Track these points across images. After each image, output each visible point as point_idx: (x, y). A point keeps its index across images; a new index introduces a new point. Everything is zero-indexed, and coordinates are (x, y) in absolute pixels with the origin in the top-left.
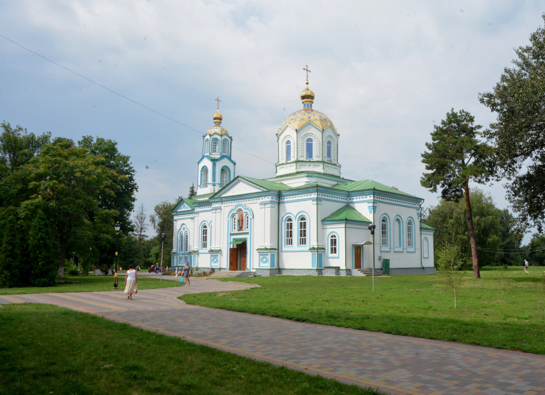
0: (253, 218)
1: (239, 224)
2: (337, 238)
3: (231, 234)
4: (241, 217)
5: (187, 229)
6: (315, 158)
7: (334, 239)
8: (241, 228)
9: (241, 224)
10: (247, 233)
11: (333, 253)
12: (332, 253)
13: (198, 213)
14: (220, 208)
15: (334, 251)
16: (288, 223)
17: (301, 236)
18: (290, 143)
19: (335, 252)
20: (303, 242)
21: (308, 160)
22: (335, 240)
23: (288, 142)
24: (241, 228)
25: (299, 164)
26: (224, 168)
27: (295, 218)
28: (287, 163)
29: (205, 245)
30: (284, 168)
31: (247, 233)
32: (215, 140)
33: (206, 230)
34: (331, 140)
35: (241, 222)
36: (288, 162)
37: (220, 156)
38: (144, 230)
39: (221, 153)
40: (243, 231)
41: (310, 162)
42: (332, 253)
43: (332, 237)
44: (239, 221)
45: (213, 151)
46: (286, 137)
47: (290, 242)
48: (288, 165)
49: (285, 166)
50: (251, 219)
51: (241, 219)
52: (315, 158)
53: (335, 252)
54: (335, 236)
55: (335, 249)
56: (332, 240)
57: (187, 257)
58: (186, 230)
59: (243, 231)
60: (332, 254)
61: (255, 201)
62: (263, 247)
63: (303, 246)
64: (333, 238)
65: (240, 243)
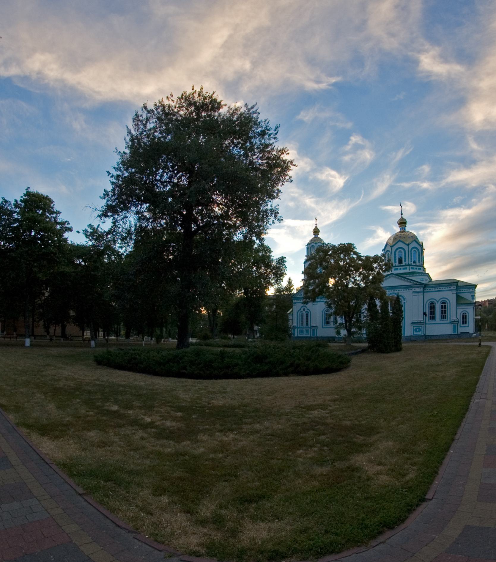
2: (467, 315)
5: (308, 309)
12: (463, 323)
15: (464, 322)
16: (431, 306)
19: (466, 323)
22: (466, 316)
27: (438, 302)
42: (463, 323)
43: (463, 314)
48: (402, 267)
49: (399, 268)
53: (466, 323)
56: (463, 316)
57: (308, 330)
58: (306, 310)
62: (417, 322)
64: (464, 315)
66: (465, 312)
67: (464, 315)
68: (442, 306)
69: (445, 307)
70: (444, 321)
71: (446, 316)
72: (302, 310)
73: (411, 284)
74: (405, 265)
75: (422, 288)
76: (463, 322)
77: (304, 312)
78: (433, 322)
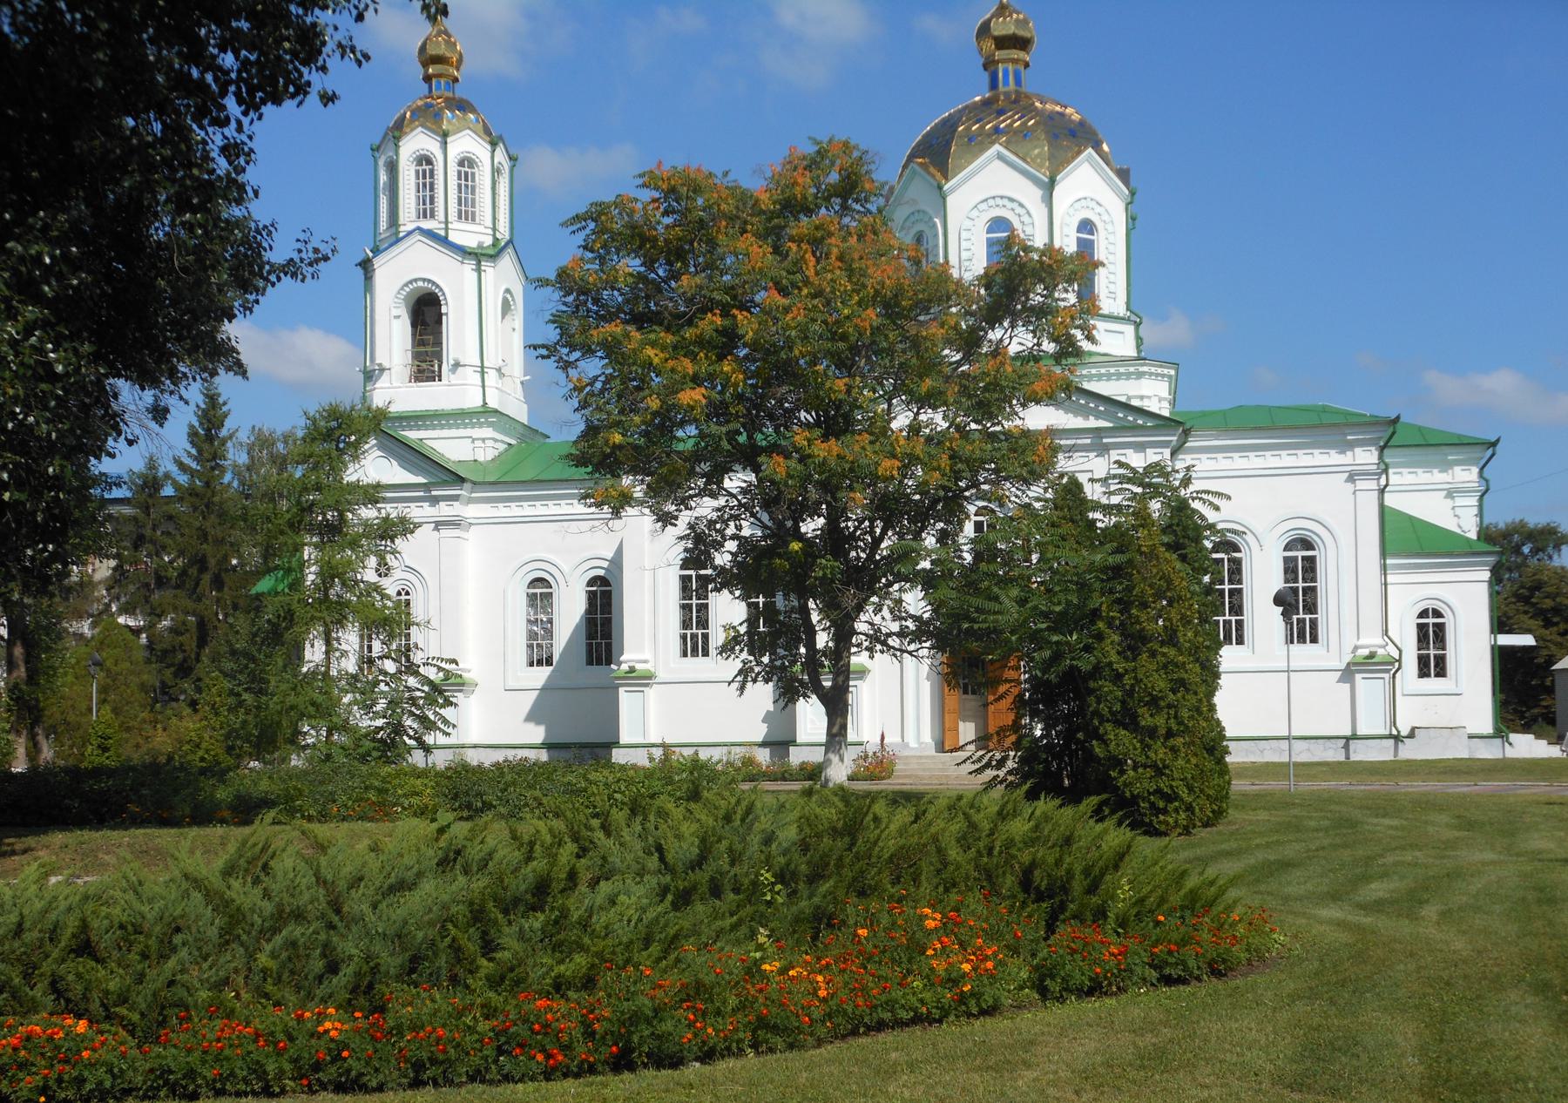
2: (1448, 620)
11: (1428, 675)
12: (1423, 672)
15: (1433, 665)
19: (1441, 672)
20: (1303, 630)
22: (1440, 628)
42: (1423, 672)
43: (1424, 614)
53: (1441, 672)
54: (1437, 614)
56: (1422, 628)
64: (1431, 621)
67: (1431, 621)
70: (1303, 653)
73: (1093, 423)
75: (1167, 452)
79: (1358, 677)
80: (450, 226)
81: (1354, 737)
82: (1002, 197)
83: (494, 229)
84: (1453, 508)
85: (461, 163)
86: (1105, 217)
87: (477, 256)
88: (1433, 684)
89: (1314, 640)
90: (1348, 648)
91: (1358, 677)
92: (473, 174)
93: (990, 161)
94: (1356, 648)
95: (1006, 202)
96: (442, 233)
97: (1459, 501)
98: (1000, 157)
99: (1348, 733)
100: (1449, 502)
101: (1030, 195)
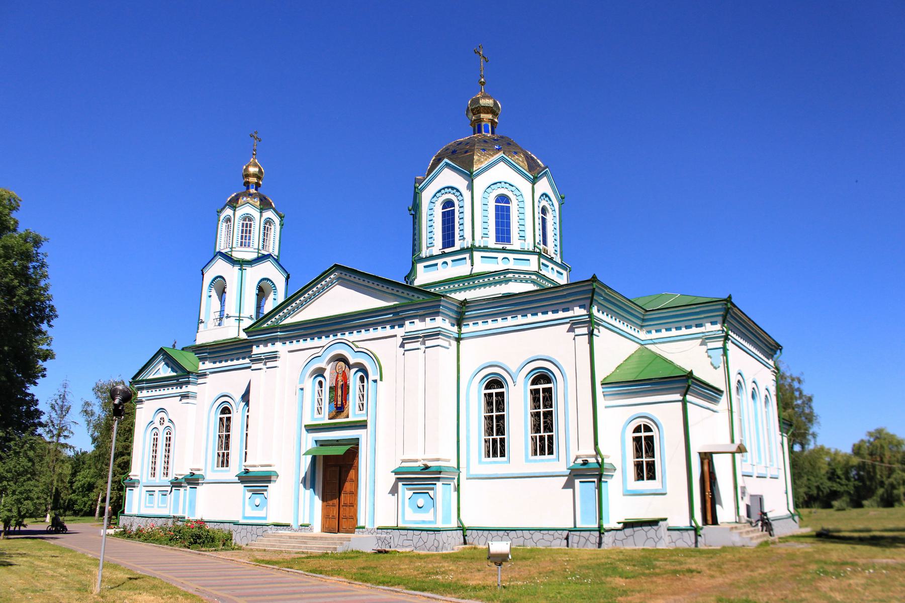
0: (381, 380)
1: (332, 399)
2: (655, 433)
3: (311, 429)
4: (340, 378)
6: (516, 244)
7: (646, 437)
8: (340, 409)
9: (339, 399)
10: (362, 425)
11: (643, 479)
12: (640, 477)
13: (204, 375)
14: (273, 357)
17: (537, 429)
18: (453, 205)
19: (652, 477)
21: (500, 246)
22: (650, 440)
23: (448, 204)
24: (340, 409)
25: (477, 255)
26: (263, 284)
28: (444, 255)
29: (224, 461)
30: (436, 265)
31: (362, 425)
32: (245, 220)
33: (229, 419)
34: (548, 207)
35: (340, 392)
36: (447, 250)
37: (255, 256)
38: (66, 433)
39: (258, 249)
40: (348, 417)
41: (504, 250)
42: (640, 477)
43: (637, 429)
44: (333, 389)
45: (239, 244)
46: (443, 191)
47: (497, 448)
48: (448, 259)
49: (440, 261)
50: (375, 381)
51: (340, 383)
52: (516, 244)
53: (652, 477)
54: (648, 429)
55: (651, 466)
56: (637, 440)
58: (167, 423)
59: (348, 417)
60: (641, 482)
61: (388, 331)
63: (543, 460)
64: (643, 434)
65: (340, 451)
66: (642, 422)
67: (643, 434)
68: (535, 393)
69: (500, 405)
70: (545, 464)
71: (551, 438)
72: (157, 424)
74: (462, 250)
76: (639, 466)
77: (161, 428)
78: (496, 465)
79: (577, 481)
80: (233, 249)
81: (575, 530)
82: (444, 189)
83: (258, 249)
84: (707, 352)
85: (266, 224)
86: (518, 193)
87: (242, 264)
88: (646, 485)
89: (503, 455)
90: (572, 459)
91: (577, 481)
92: (251, 224)
93: (442, 169)
94: (577, 458)
95: (450, 190)
96: (230, 253)
97: (711, 345)
98: (447, 165)
99: (572, 526)
100: (704, 348)
101: (460, 183)
